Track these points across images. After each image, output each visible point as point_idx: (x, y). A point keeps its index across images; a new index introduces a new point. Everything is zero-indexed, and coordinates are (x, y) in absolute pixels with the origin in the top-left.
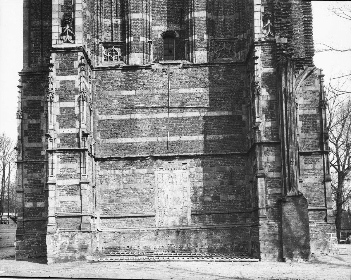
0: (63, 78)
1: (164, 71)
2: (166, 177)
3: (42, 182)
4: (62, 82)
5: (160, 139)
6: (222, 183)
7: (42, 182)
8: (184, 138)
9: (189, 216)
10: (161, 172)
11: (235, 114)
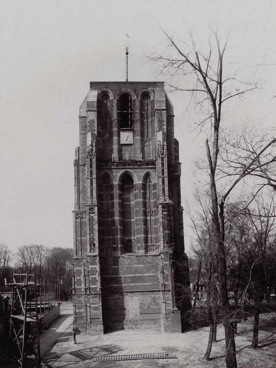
0: (92, 266)
1: (128, 258)
2: (130, 299)
3: (82, 302)
4: (91, 268)
5: (127, 285)
6: (151, 302)
7: (82, 302)
8: (136, 284)
9: (139, 314)
10: (128, 297)
11: (155, 275)
